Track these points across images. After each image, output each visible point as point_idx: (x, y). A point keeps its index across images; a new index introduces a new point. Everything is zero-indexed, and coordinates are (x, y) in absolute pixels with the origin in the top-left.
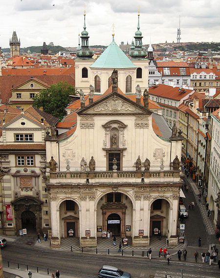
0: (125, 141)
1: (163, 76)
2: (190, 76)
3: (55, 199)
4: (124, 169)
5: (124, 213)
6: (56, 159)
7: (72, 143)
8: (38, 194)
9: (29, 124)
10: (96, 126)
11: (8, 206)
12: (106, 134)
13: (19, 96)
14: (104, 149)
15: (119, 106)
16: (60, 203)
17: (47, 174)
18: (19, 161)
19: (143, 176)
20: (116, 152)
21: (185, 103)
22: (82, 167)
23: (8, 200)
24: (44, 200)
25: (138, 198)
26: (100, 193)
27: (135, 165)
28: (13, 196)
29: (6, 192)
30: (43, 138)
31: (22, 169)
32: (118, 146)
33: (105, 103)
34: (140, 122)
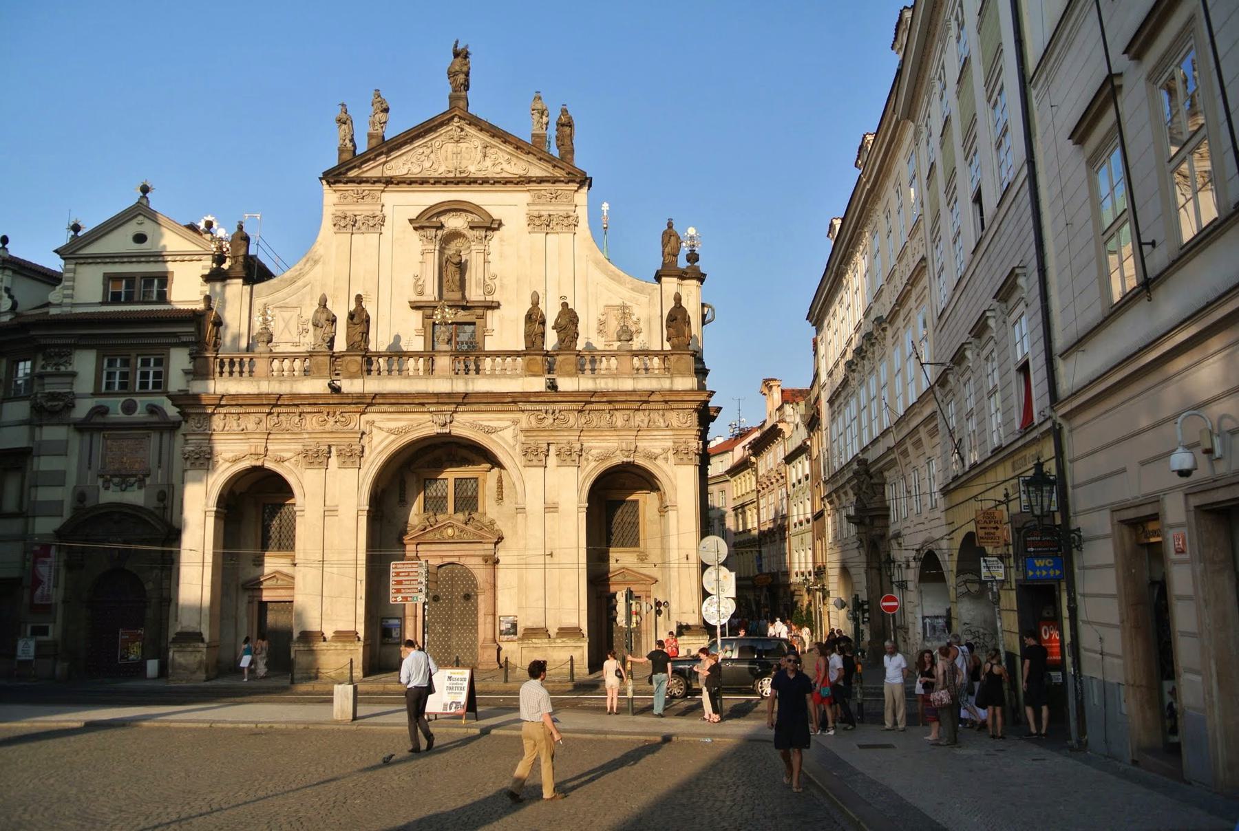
0: (494, 277)
7: (300, 283)
14: (416, 307)
18: (110, 375)
19: (550, 371)
22: (319, 330)
23: (45, 526)
25: (534, 455)
29: (45, 494)
33: (421, 150)
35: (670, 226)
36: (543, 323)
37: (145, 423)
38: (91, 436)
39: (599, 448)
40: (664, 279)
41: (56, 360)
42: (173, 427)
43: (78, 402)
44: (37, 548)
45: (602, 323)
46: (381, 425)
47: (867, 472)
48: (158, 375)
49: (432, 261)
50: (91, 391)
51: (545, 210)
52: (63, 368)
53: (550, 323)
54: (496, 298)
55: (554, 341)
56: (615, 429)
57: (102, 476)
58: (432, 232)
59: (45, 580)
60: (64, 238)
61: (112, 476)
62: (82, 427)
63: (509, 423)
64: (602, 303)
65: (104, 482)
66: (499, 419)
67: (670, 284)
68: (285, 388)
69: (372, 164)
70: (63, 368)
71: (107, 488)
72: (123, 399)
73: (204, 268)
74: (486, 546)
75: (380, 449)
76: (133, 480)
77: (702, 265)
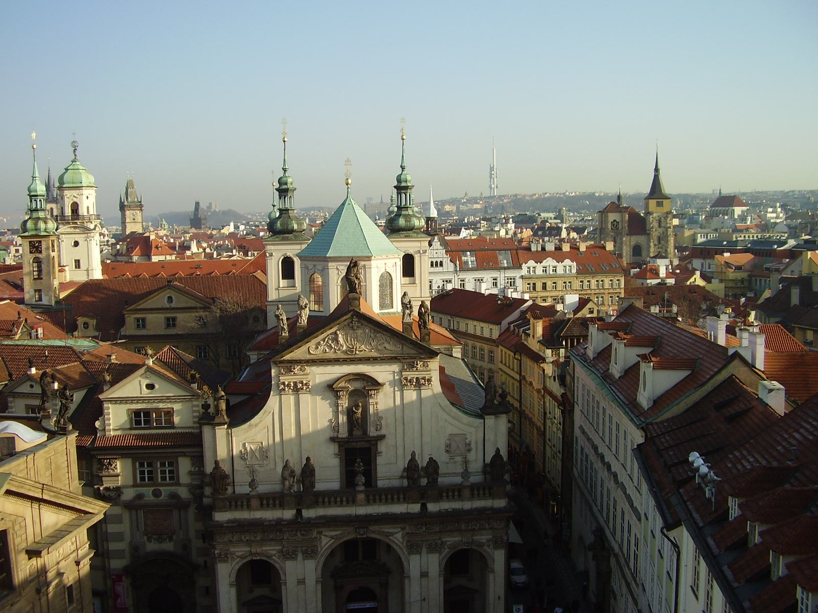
1: (464, 268)
2: (520, 267)
3: (225, 558)
4: (381, 484)
6: (226, 468)
9: (163, 389)
11: (119, 578)
13: (141, 323)
14: (333, 439)
16: (237, 567)
17: (206, 501)
18: (142, 472)
20: (359, 445)
21: (512, 328)
23: (117, 564)
24: (201, 560)
25: (414, 548)
26: (326, 541)
27: (405, 474)
28: (127, 554)
29: (113, 546)
30: (194, 417)
31: (148, 491)
32: (365, 432)
38: (136, 511)
39: (451, 541)
40: (486, 417)
45: (448, 446)
46: (327, 534)
50: (131, 483)
54: (383, 432)
57: (146, 535)
65: (147, 538)
66: (395, 528)
71: (150, 542)
72: (153, 488)
75: (326, 547)
76: (165, 536)
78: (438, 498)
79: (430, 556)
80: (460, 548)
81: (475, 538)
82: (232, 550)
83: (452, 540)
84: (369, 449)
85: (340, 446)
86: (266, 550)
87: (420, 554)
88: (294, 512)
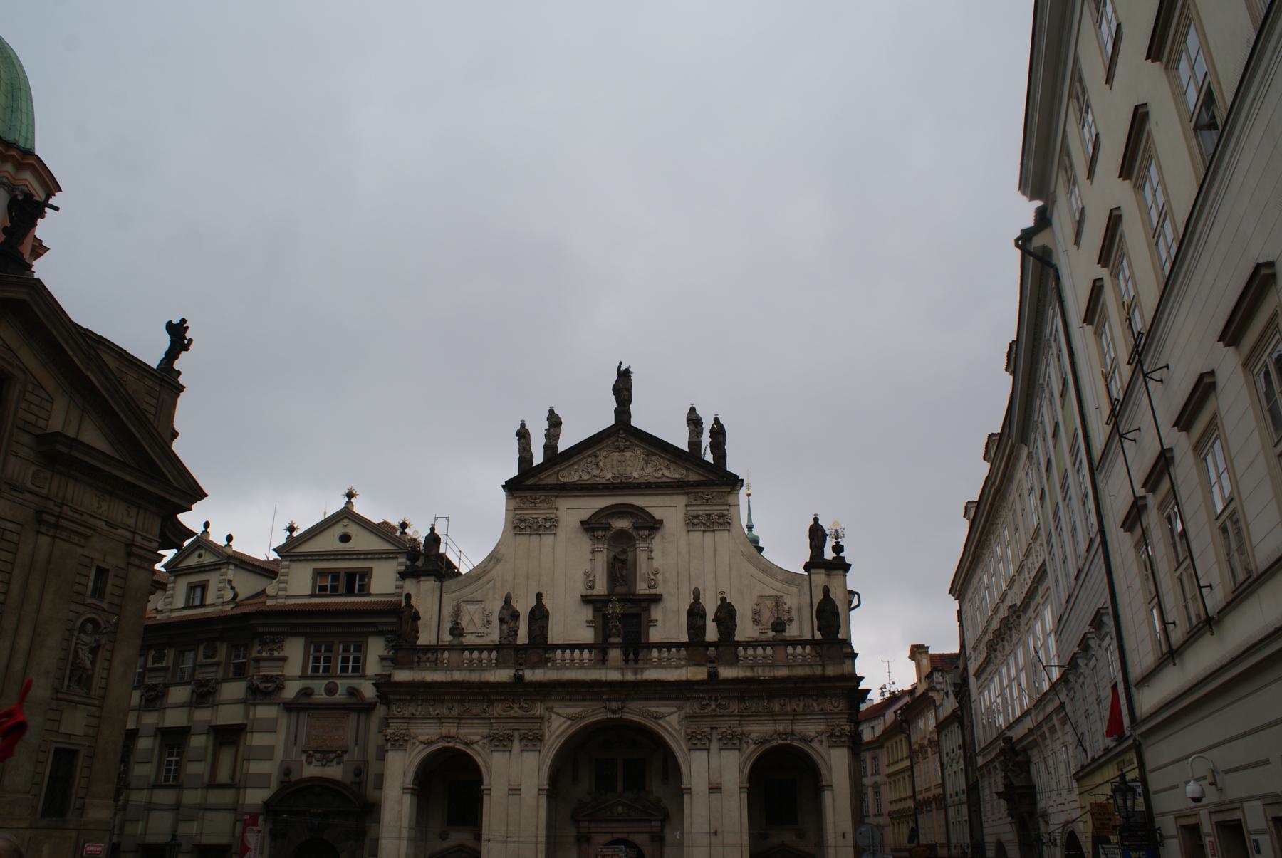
3: (400, 742)
5: (659, 839)
7: (484, 579)
8: (358, 772)
10: (562, 525)
11: (254, 820)
12: (593, 552)
14: (586, 600)
15: (636, 466)
18: (317, 660)
19: (712, 662)
22: (504, 627)
23: (255, 797)
25: (697, 741)
26: (559, 724)
29: (255, 767)
31: (319, 686)
33: (590, 459)
34: (702, 510)
35: (816, 520)
36: (703, 616)
37: (345, 704)
41: (271, 646)
42: (368, 708)
43: (289, 684)
44: (247, 817)
45: (756, 613)
46: (560, 711)
47: (1013, 749)
48: (356, 660)
49: (602, 559)
51: (702, 510)
52: (276, 654)
53: (710, 614)
55: (712, 633)
56: (772, 714)
57: (305, 752)
58: (600, 533)
59: (252, 847)
60: (281, 539)
61: (315, 752)
62: (290, 707)
63: (674, 709)
64: (756, 593)
67: (820, 577)
68: (474, 677)
69: (548, 473)
70: (276, 654)
71: (310, 763)
72: (326, 682)
73: (400, 564)
74: (654, 823)
75: (558, 732)
76: (332, 756)
77: (847, 555)
78: (734, 661)
79: (724, 753)
80: (773, 744)
81: (800, 728)
82: (413, 730)
83: (758, 729)
84: (638, 616)
85: (596, 610)
86: (465, 734)
87: (708, 750)
88: (512, 672)
